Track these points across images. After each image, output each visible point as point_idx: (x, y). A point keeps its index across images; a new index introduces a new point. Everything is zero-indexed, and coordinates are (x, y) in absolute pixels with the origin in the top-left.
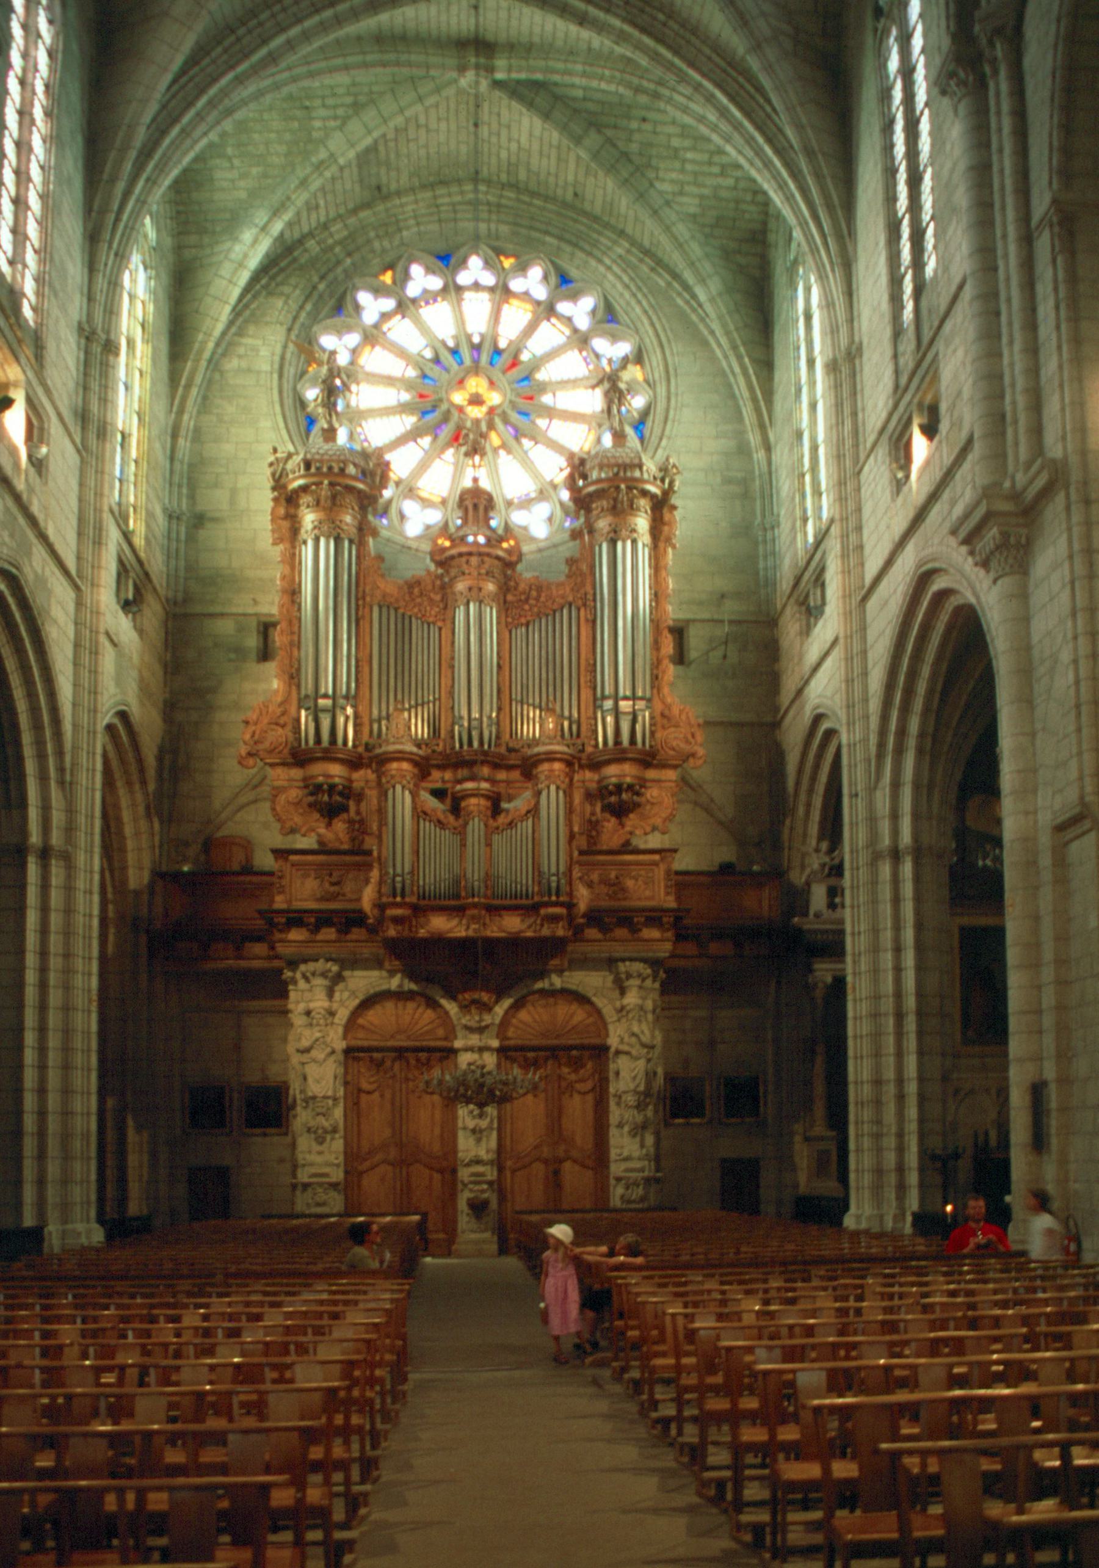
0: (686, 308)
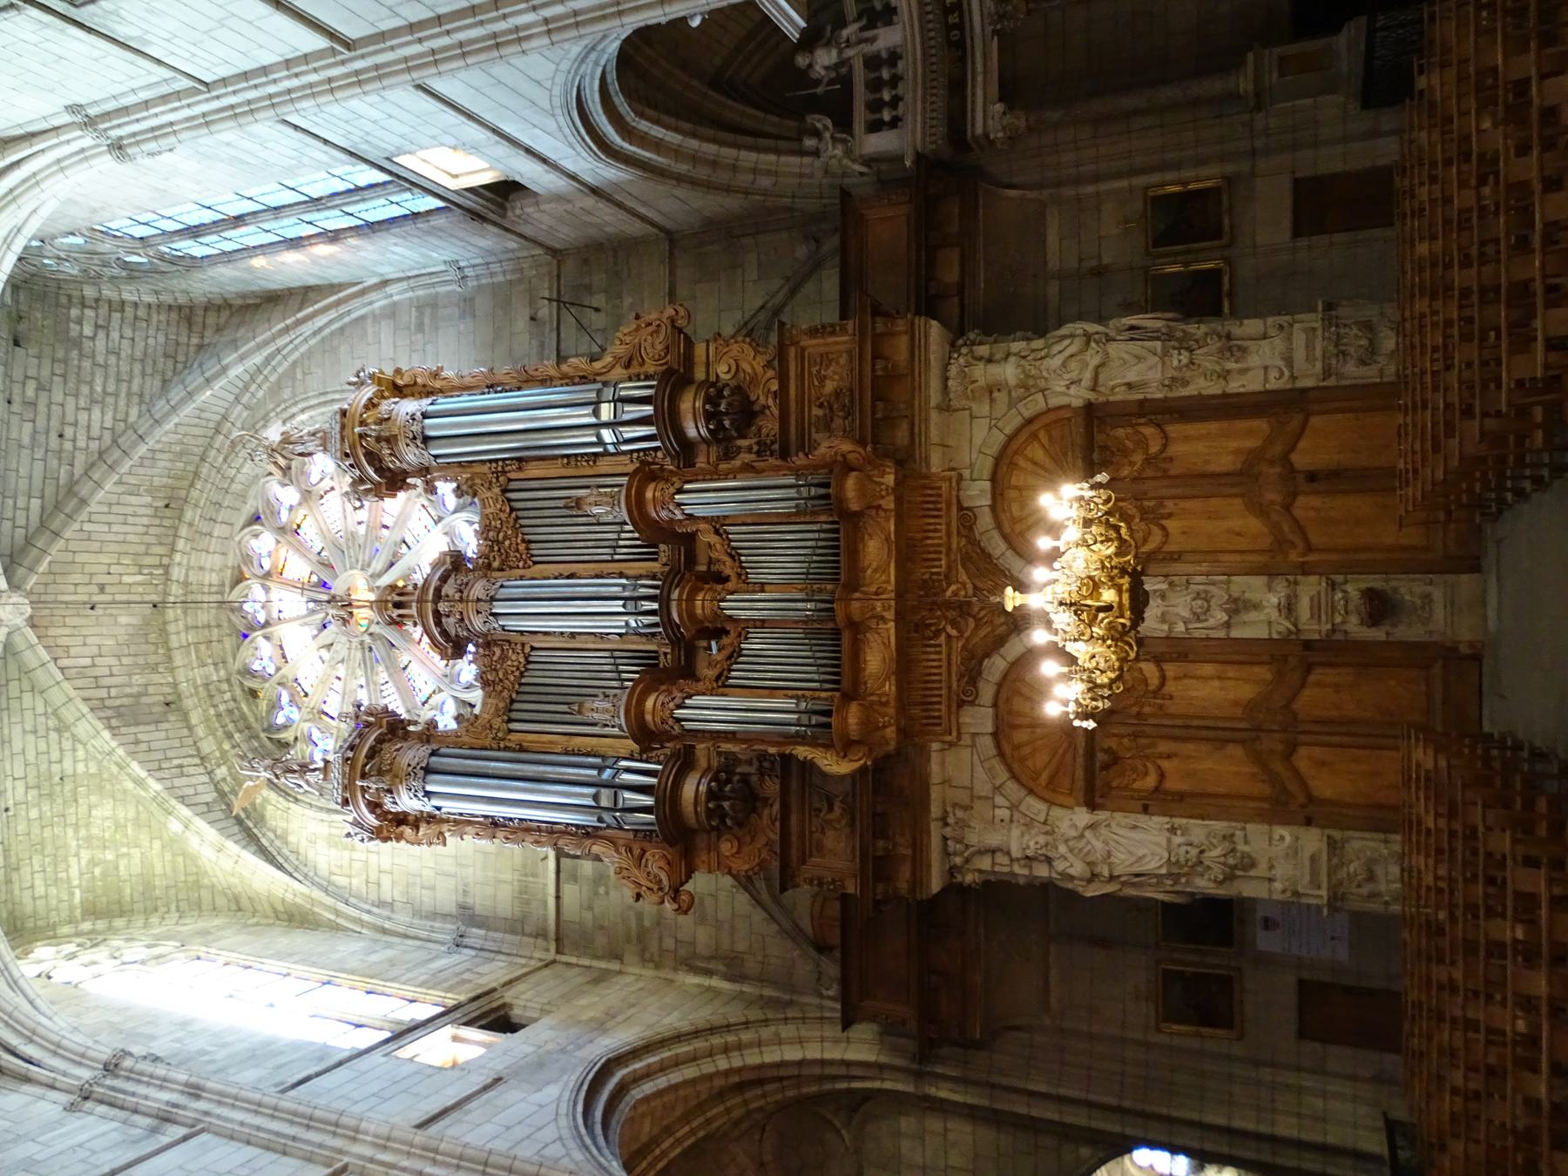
0: (265, 387)
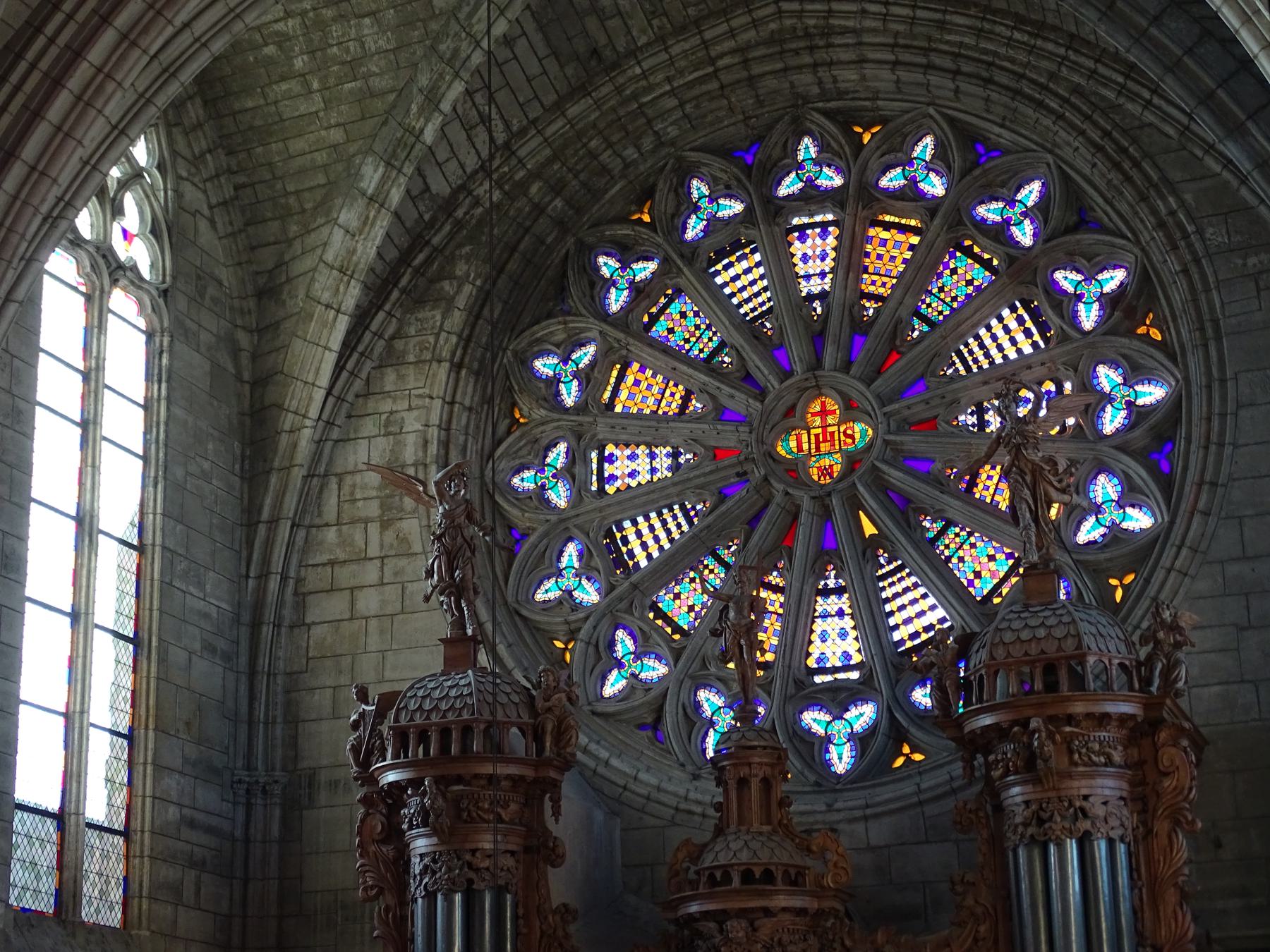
0: (1226, 175)
